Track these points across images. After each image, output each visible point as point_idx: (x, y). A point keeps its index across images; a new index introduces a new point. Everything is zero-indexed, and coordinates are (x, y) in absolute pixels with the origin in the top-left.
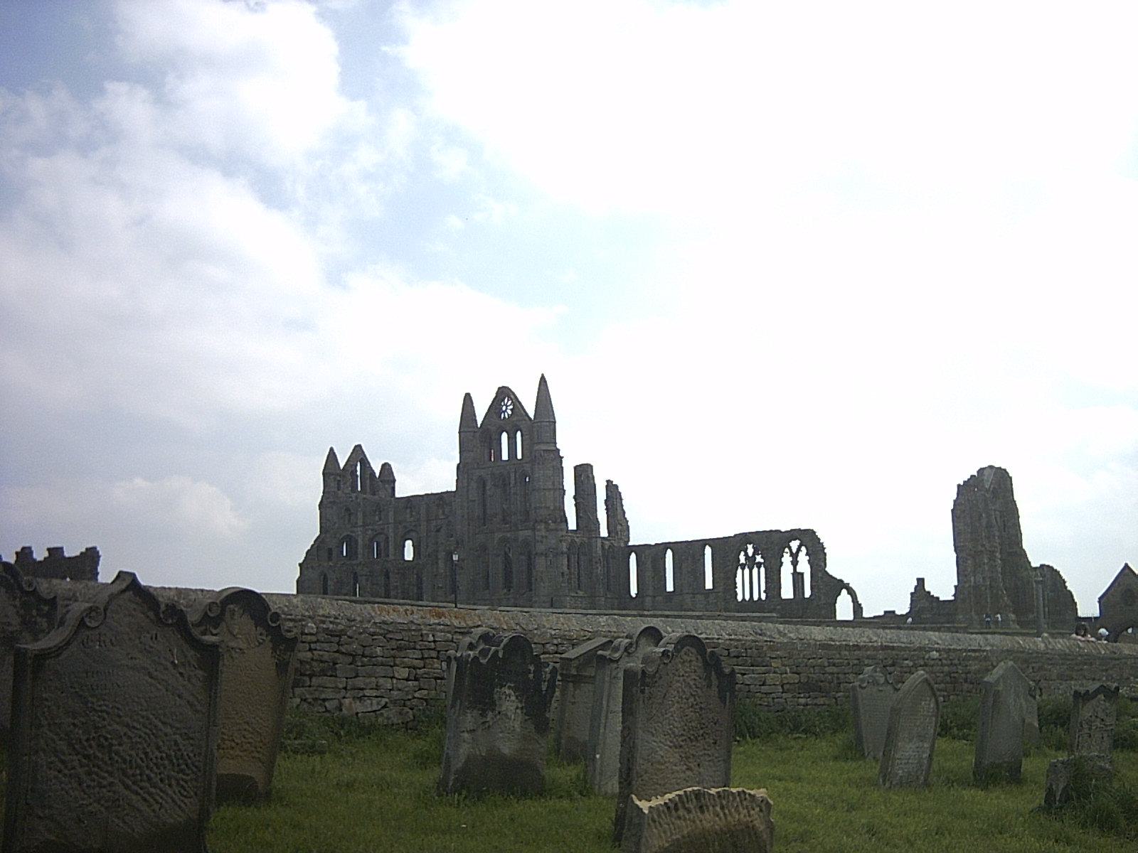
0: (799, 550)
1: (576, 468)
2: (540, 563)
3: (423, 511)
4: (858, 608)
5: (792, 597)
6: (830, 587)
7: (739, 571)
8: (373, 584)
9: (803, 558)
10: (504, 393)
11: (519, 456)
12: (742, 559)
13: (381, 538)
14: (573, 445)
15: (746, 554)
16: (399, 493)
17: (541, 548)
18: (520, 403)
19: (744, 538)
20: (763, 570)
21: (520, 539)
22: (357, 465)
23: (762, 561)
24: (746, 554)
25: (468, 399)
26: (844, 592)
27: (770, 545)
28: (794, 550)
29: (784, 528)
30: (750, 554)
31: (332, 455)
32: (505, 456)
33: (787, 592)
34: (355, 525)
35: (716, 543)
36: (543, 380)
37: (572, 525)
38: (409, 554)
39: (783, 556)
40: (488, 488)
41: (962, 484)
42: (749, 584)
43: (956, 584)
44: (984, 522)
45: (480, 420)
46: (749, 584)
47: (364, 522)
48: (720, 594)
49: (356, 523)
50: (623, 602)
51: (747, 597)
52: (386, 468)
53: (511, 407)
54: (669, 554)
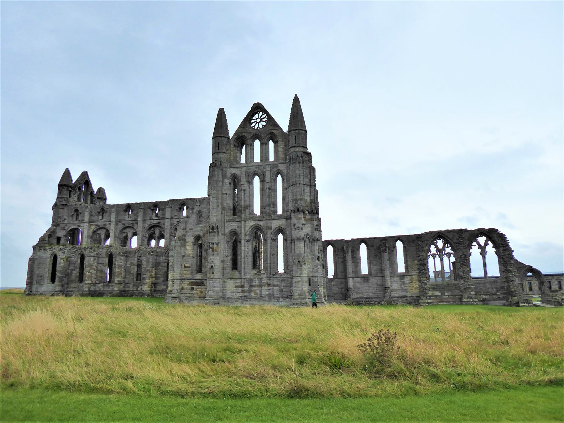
0: (486, 244)
7: (431, 260)
8: (98, 264)
9: (490, 249)
11: (272, 158)
12: (433, 249)
15: (436, 247)
21: (273, 228)
23: (452, 252)
24: (436, 247)
27: (460, 241)
28: (482, 244)
29: (472, 227)
34: (82, 221)
35: (407, 240)
36: (296, 101)
39: (471, 248)
47: (89, 220)
48: (414, 277)
49: (84, 220)
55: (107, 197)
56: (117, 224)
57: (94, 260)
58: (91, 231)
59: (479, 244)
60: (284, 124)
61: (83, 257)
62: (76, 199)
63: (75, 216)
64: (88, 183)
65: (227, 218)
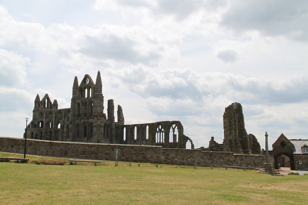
0: (175, 127)
1: (109, 101)
2: (95, 129)
3: (64, 114)
4: (193, 146)
5: (172, 142)
6: (184, 139)
7: (157, 133)
8: (47, 135)
9: (176, 130)
10: (87, 77)
11: (90, 96)
13: (51, 121)
14: (107, 94)
15: (159, 128)
17: (95, 124)
18: (92, 80)
19: (158, 124)
20: (164, 133)
22: (46, 100)
23: (164, 130)
24: (159, 128)
25: (76, 78)
26: (189, 140)
27: (167, 125)
28: (174, 128)
30: (160, 129)
31: (38, 97)
32: (86, 96)
33: (171, 140)
34: (43, 118)
36: (99, 73)
38: (59, 126)
40: (81, 105)
41: (227, 107)
42: (159, 138)
43: (224, 139)
44: (233, 119)
45: (79, 85)
46: (159, 138)
50: (122, 141)
51: (159, 142)
52: (55, 101)
53: (89, 81)
54: (136, 127)
55: (58, 104)
57: (45, 134)
58: (47, 121)
59: (173, 127)
61: (42, 133)
63: (41, 115)
64: (48, 99)
65: (76, 119)
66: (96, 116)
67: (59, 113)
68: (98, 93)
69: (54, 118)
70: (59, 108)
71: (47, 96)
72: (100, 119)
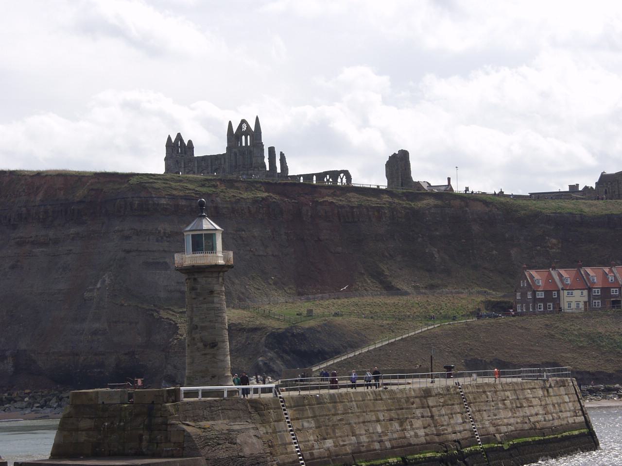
0: (343, 177)
1: (269, 148)
3: (209, 162)
10: (243, 121)
11: (249, 145)
12: (325, 180)
14: (267, 141)
15: (327, 179)
16: (196, 155)
19: (326, 173)
24: (327, 179)
25: (230, 123)
27: (335, 174)
29: (339, 170)
31: (169, 139)
34: (181, 167)
35: (317, 175)
36: (257, 119)
37: (268, 169)
40: (238, 154)
45: (235, 130)
52: (190, 142)
56: (198, 168)
60: (253, 128)
62: (176, 153)
64: (182, 141)
66: (256, 168)
67: (202, 160)
68: (258, 142)
69: (196, 168)
70: (197, 154)
71: (179, 137)
72: (261, 171)
